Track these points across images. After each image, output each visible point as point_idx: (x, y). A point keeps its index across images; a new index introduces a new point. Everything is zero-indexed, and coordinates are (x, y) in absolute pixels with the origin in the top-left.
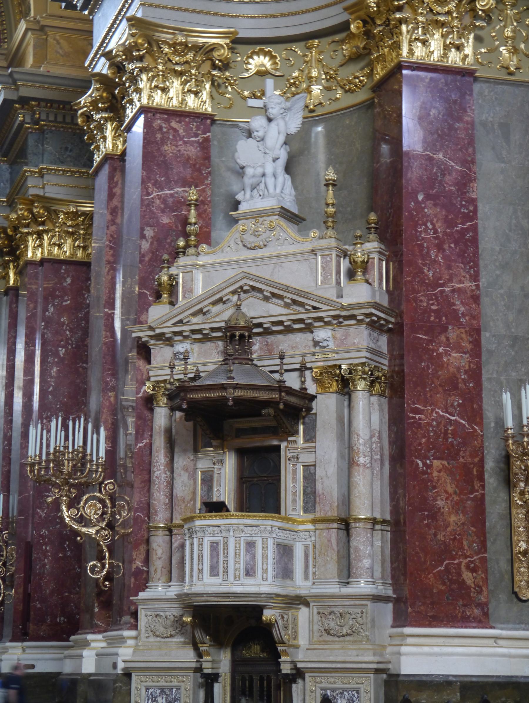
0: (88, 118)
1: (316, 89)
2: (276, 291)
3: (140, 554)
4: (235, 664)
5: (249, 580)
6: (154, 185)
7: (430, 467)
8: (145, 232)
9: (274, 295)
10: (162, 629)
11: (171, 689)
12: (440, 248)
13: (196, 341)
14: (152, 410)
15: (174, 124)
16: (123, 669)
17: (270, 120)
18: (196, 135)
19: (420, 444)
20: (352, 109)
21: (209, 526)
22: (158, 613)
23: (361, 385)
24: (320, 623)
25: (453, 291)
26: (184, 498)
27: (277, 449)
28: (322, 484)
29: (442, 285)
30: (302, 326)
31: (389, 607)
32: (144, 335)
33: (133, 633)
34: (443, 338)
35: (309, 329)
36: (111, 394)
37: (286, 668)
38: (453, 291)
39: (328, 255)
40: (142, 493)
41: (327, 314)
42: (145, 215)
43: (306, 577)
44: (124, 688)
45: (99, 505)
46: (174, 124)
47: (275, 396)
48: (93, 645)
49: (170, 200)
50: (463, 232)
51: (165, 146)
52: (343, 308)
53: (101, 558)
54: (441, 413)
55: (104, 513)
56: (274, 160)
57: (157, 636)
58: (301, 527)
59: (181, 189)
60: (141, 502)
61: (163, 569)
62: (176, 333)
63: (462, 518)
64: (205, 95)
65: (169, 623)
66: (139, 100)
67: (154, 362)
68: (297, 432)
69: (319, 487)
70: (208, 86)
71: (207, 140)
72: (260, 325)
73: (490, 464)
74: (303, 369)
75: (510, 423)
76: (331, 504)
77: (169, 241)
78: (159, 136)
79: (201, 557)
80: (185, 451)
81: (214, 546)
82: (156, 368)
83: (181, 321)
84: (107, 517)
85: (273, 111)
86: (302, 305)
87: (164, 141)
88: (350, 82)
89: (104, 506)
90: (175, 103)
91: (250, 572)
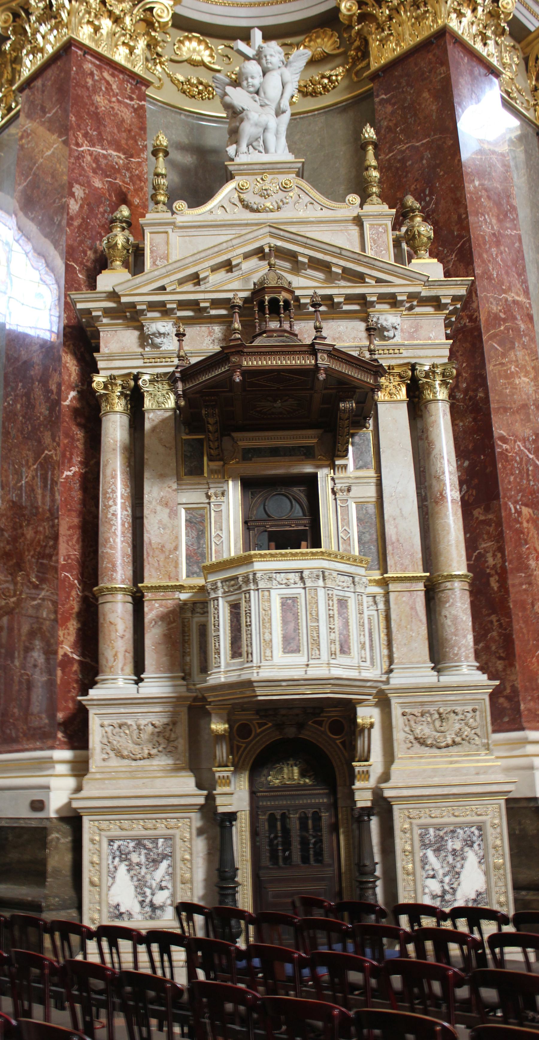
2: (320, 256)
3: (69, 634)
5: (342, 660)
8: (74, 190)
10: (131, 746)
11: (155, 840)
16: (58, 811)
18: (131, 99)
19: (509, 482)
20: (316, 113)
21: (279, 572)
22: (125, 721)
24: (407, 729)
26: (163, 546)
28: (396, 527)
39: (380, 225)
40: (70, 543)
42: (74, 169)
44: (62, 840)
49: (103, 162)
51: (97, 97)
54: (522, 448)
57: (123, 757)
59: (115, 153)
60: (69, 556)
61: (127, 654)
62: (152, 306)
65: (144, 736)
76: (412, 555)
77: (101, 210)
80: (162, 476)
83: (163, 288)
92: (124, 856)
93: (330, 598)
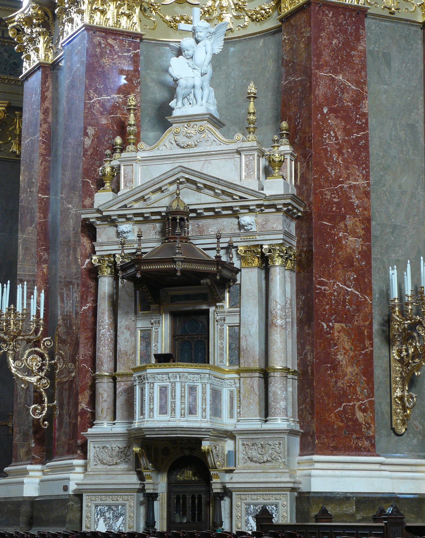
0: (19, 31)
1: (228, 17)
2: (208, 183)
3: (85, 398)
4: (170, 485)
5: (192, 418)
6: (95, 91)
7: (332, 328)
8: (87, 131)
9: (206, 186)
10: (108, 458)
11: (117, 506)
12: (340, 152)
13: (137, 222)
14: (96, 280)
15: (110, 41)
16: (74, 491)
17: (197, 42)
18: (129, 51)
19: (325, 310)
20: (258, 35)
21: (158, 374)
22: (105, 445)
23: (278, 262)
24: (244, 453)
25: (350, 187)
26: (126, 352)
27: (207, 312)
28: (246, 341)
29: (342, 182)
30: (230, 212)
31: (297, 440)
32: (92, 216)
33: (81, 462)
34: (342, 225)
35: (235, 214)
36: (45, 266)
37: (216, 488)
38: (350, 187)
39: (251, 155)
40: (86, 348)
41: (252, 203)
42: (88, 116)
43: (232, 416)
44: (75, 506)
45: (39, 359)
46: (110, 41)
47: (214, 269)
48: (31, 474)
50: (357, 140)
51: (104, 59)
52: (266, 198)
53: (40, 401)
54: (341, 286)
55: (43, 365)
56: (202, 75)
57: (104, 464)
58: (227, 376)
59: (116, 96)
60: (85, 355)
61: (108, 410)
62: (120, 216)
63: (356, 370)
64: (135, 19)
65: (114, 453)
66: (82, 20)
67: (99, 240)
68: (222, 299)
69: (243, 343)
70: (138, 10)
71: (137, 55)
72: (194, 211)
73: (376, 327)
74: (229, 248)
75: (395, 294)
76: (253, 357)
77: (107, 138)
78: (98, 50)
79: (151, 399)
80: (127, 313)
81: (163, 390)
82: (102, 245)
83: (125, 206)
84: (46, 368)
85: (200, 35)
86: (230, 195)
87: (103, 54)
88: (257, 13)
89: (43, 359)
90: (111, 23)
91: (192, 411)
92: (102, 514)
93: (182, 387)
